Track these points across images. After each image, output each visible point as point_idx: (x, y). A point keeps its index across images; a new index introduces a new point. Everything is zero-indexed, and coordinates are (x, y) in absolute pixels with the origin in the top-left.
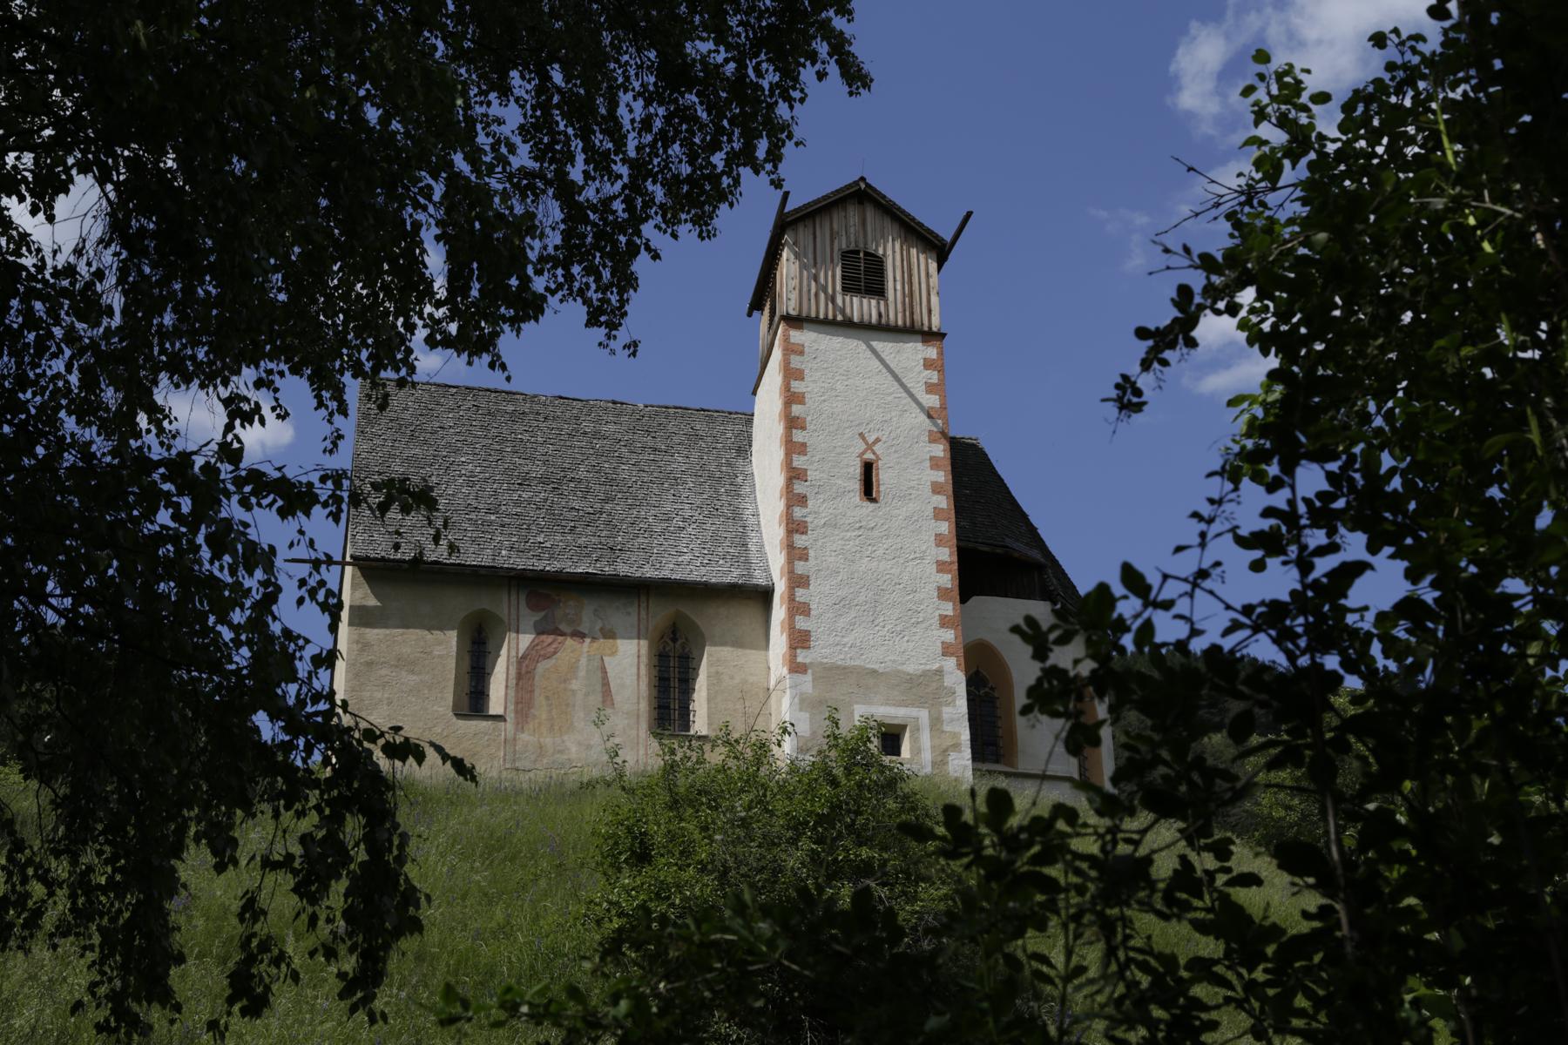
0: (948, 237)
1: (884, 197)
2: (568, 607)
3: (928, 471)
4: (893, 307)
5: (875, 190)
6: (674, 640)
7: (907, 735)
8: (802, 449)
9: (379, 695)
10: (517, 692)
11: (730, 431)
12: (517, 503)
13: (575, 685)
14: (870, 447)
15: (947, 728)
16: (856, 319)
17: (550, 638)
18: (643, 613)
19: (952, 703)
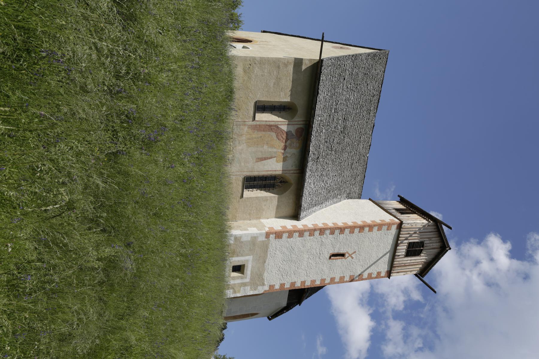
0: (425, 279)
1: (442, 256)
2: (297, 143)
3: (339, 276)
4: (401, 259)
5: (446, 253)
6: (281, 182)
7: (240, 275)
8: (352, 232)
9: (266, 71)
10: (264, 125)
11: (357, 189)
12: (338, 119)
13: (266, 147)
14: (350, 255)
15: (242, 288)
16: (398, 248)
17: (284, 137)
18: (292, 172)
19: (251, 289)
